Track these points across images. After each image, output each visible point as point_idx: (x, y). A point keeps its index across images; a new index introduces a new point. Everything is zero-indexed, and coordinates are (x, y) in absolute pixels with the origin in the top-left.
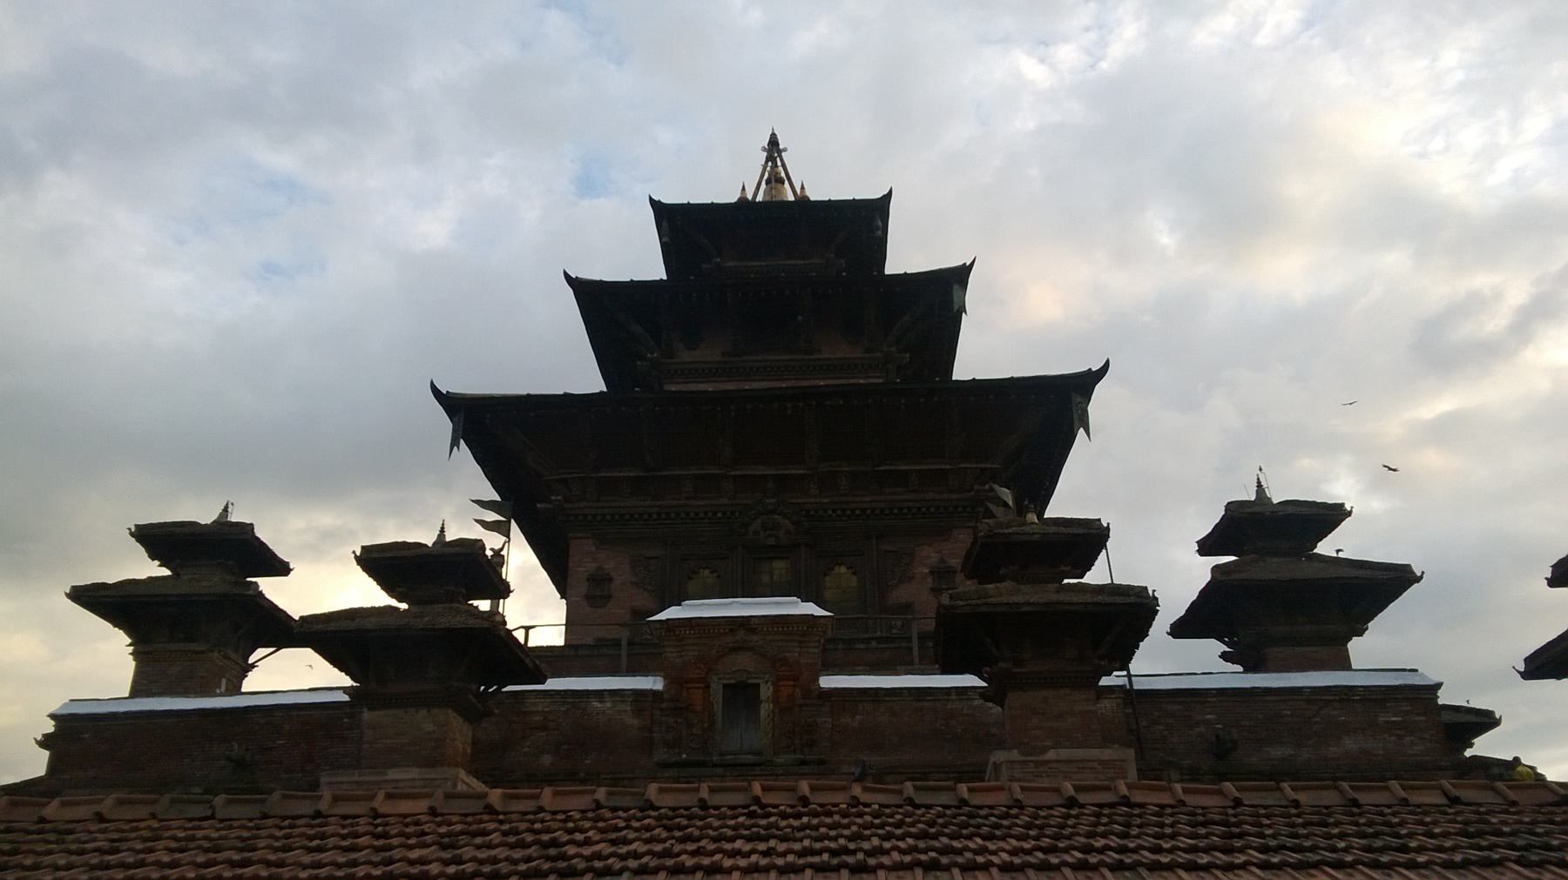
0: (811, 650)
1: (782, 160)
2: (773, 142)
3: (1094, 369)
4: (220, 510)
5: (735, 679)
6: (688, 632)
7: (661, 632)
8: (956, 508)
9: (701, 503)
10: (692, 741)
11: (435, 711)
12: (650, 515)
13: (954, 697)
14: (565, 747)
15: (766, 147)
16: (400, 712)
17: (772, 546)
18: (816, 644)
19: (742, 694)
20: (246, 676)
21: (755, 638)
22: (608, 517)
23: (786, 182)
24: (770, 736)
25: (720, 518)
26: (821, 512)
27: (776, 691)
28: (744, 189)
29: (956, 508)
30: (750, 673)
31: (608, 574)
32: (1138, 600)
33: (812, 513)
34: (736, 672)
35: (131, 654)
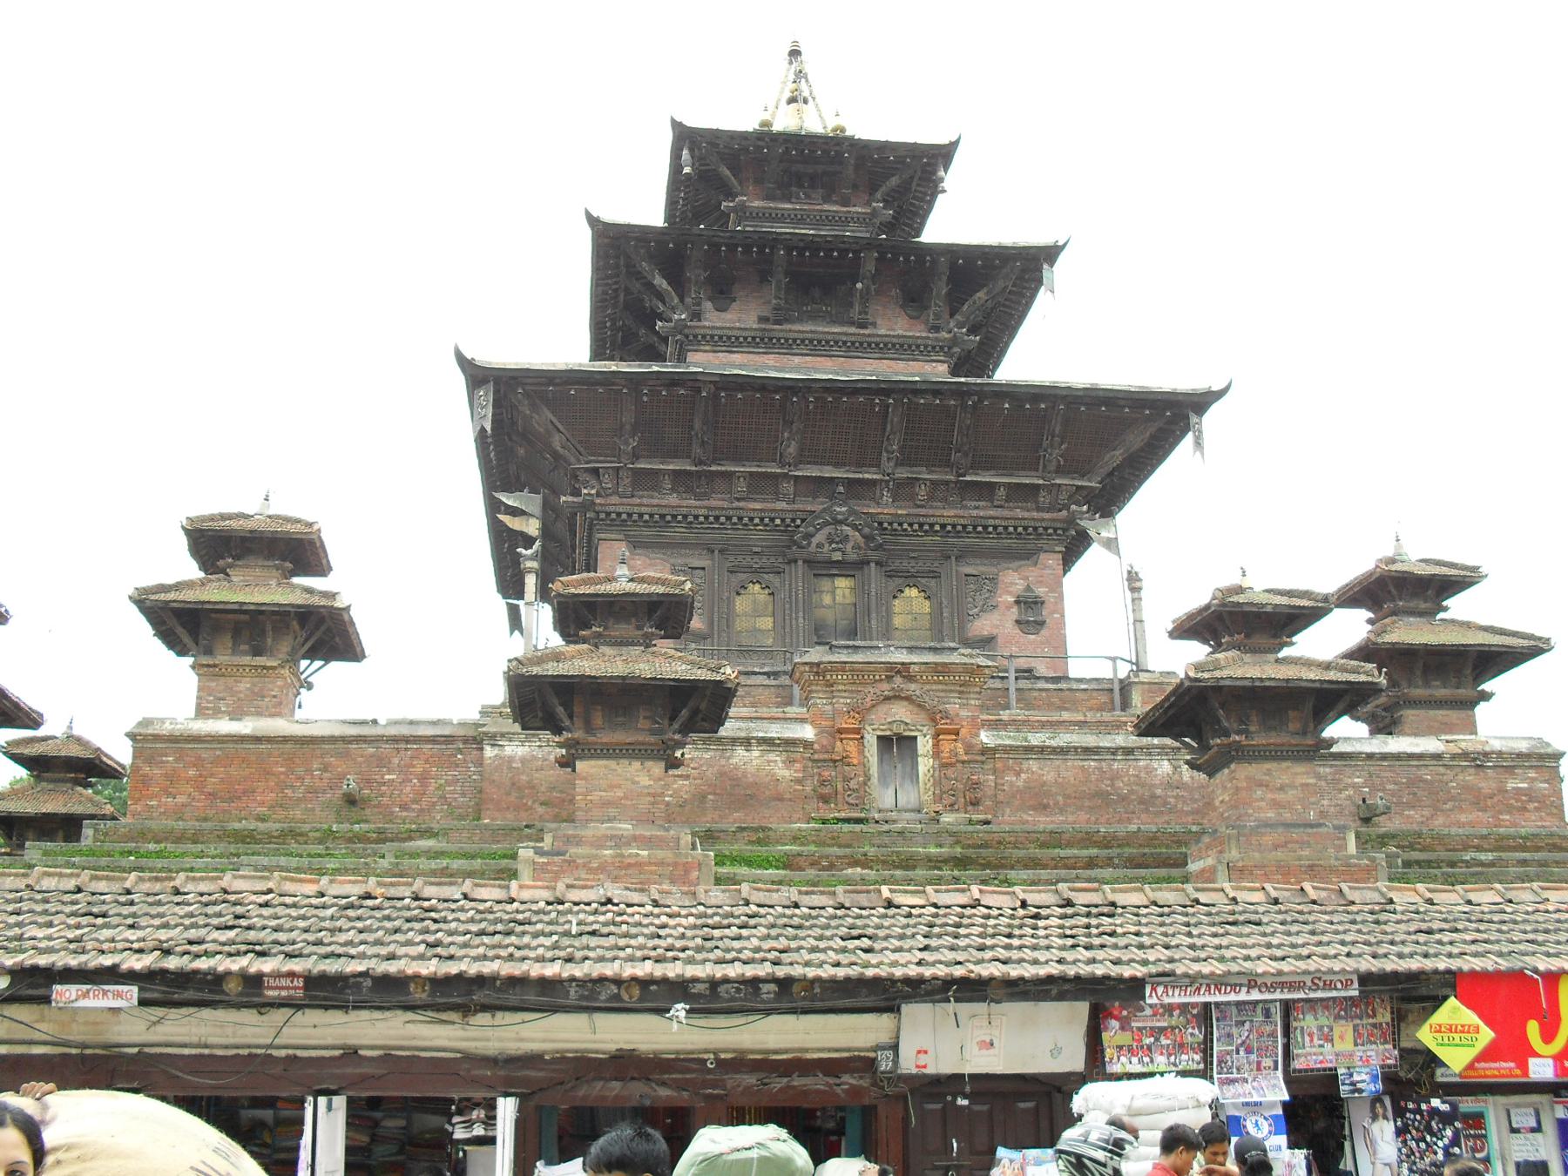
0: (973, 702)
2: (795, 53)
3: (1214, 389)
5: (891, 730)
6: (840, 677)
8: (1046, 529)
10: (849, 795)
11: (649, 764)
12: (696, 517)
14: (710, 797)
16: (612, 764)
17: (838, 562)
18: (977, 696)
19: (897, 745)
21: (913, 686)
22: (646, 517)
24: (931, 793)
25: (777, 525)
26: (895, 525)
27: (936, 745)
30: (906, 724)
33: (886, 525)
34: (890, 723)
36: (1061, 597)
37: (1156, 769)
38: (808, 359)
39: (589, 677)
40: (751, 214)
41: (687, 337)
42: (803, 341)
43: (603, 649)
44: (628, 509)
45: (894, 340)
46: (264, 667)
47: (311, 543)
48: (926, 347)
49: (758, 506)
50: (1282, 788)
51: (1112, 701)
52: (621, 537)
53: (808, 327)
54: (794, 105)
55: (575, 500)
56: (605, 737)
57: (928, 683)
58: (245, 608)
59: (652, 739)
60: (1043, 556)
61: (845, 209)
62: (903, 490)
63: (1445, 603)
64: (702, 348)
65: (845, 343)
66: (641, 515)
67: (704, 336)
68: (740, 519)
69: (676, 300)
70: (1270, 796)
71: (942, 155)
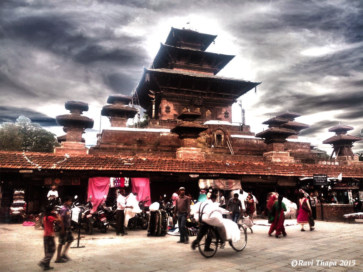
9: (186, 95)
11: (195, 139)
12: (178, 97)
16: (190, 139)
19: (219, 137)
21: (222, 128)
22: (170, 96)
27: (225, 136)
29: (230, 102)
36: (231, 113)
38: (192, 71)
44: (167, 95)
49: (187, 96)
50: (279, 147)
51: (240, 130)
52: (165, 99)
53: (193, 66)
55: (159, 93)
56: (189, 135)
57: (224, 127)
59: (195, 135)
60: (229, 106)
62: (209, 95)
63: (294, 119)
66: (169, 96)
68: (184, 97)
70: (278, 148)
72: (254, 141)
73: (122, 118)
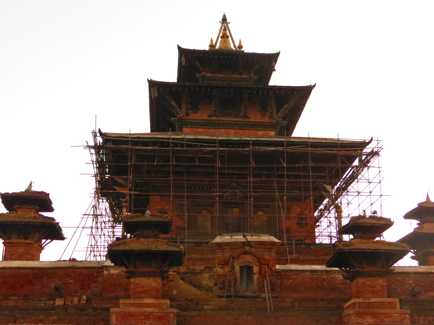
0: (273, 255)
1: (228, 27)
2: (224, 19)
3: (367, 141)
4: (29, 185)
5: (245, 264)
6: (226, 247)
7: (216, 247)
11: (156, 278)
13: (324, 274)
15: (221, 21)
20: (41, 252)
21: (252, 249)
23: (230, 39)
27: (260, 269)
28: (212, 41)
30: (250, 262)
31: (167, 212)
32: (405, 249)
34: (244, 262)
35: (3, 243)
37: (337, 278)
38: (226, 130)
39: (135, 250)
40: (207, 78)
41: (182, 123)
42: (223, 124)
43: (141, 239)
45: (256, 123)
46: (29, 243)
47: (46, 200)
48: (267, 126)
54: (223, 39)
56: (141, 270)
58: (22, 223)
59: (156, 270)
61: (240, 76)
64: (188, 127)
65: (238, 124)
67: (188, 123)
69: (179, 110)
71: (274, 57)
72: (337, 276)
73: (27, 241)
